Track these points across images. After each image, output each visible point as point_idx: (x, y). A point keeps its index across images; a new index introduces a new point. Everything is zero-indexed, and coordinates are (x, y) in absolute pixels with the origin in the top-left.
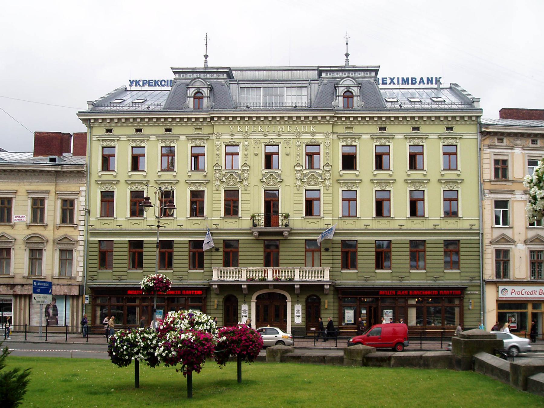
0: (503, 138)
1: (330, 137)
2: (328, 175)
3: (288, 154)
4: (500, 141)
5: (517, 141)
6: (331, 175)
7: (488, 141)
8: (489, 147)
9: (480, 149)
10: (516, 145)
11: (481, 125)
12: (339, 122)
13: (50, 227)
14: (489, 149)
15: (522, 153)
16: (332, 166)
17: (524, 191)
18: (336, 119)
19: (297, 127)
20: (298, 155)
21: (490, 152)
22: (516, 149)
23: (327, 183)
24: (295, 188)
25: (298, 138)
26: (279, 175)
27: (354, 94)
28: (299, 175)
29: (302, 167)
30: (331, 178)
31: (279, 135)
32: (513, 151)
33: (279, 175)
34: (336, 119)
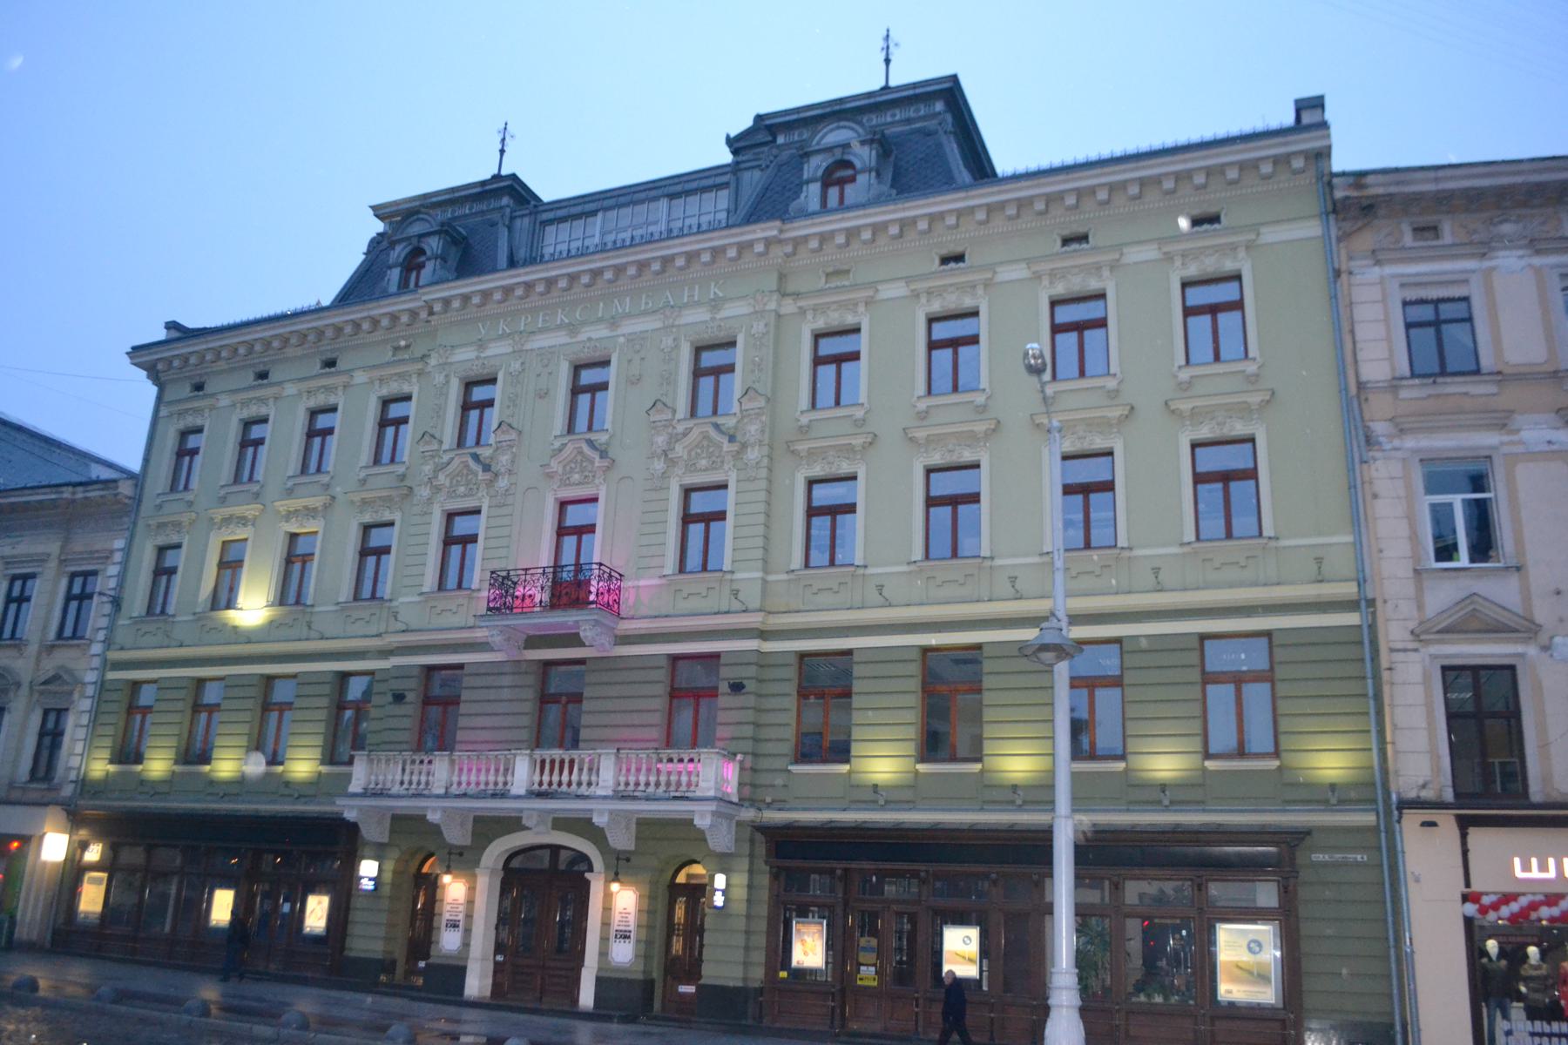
0: (1440, 221)
1: (767, 308)
4: (1427, 234)
5: (1501, 222)
7: (1366, 240)
8: (1376, 257)
9: (1337, 273)
10: (1501, 237)
11: (1328, 180)
13: (33, 649)
14: (1377, 269)
15: (1530, 265)
16: (768, 400)
17: (1558, 411)
18: (789, 249)
21: (1382, 278)
22: (1501, 253)
23: (753, 454)
27: (858, 165)
31: (613, 323)
32: (1487, 264)
34: (789, 249)
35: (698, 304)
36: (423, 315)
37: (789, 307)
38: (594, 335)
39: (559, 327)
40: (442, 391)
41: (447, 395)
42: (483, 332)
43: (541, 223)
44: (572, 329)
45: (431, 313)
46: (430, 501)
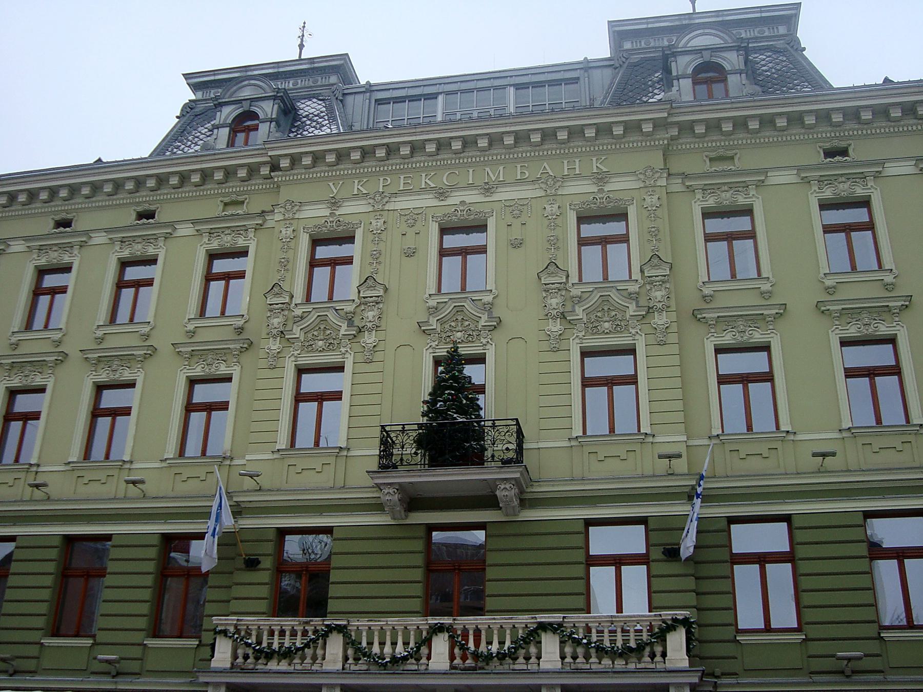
2: (658, 294)
3: (517, 244)
6: (672, 296)
12: (686, 142)
18: (674, 132)
19: (545, 164)
20: (554, 243)
23: (660, 320)
24: (545, 346)
25: (552, 197)
26: (488, 308)
27: (728, 67)
28: (554, 302)
29: (568, 277)
30: (673, 303)
31: (488, 189)
33: (488, 308)
34: (674, 132)
35: (579, 177)
36: (265, 171)
37: (677, 186)
38: (468, 200)
39: (423, 191)
40: (289, 244)
41: (295, 250)
42: (335, 191)
43: (376, 100)
44: (441, 194)
45: (275, 167)
46: (279, 355)
